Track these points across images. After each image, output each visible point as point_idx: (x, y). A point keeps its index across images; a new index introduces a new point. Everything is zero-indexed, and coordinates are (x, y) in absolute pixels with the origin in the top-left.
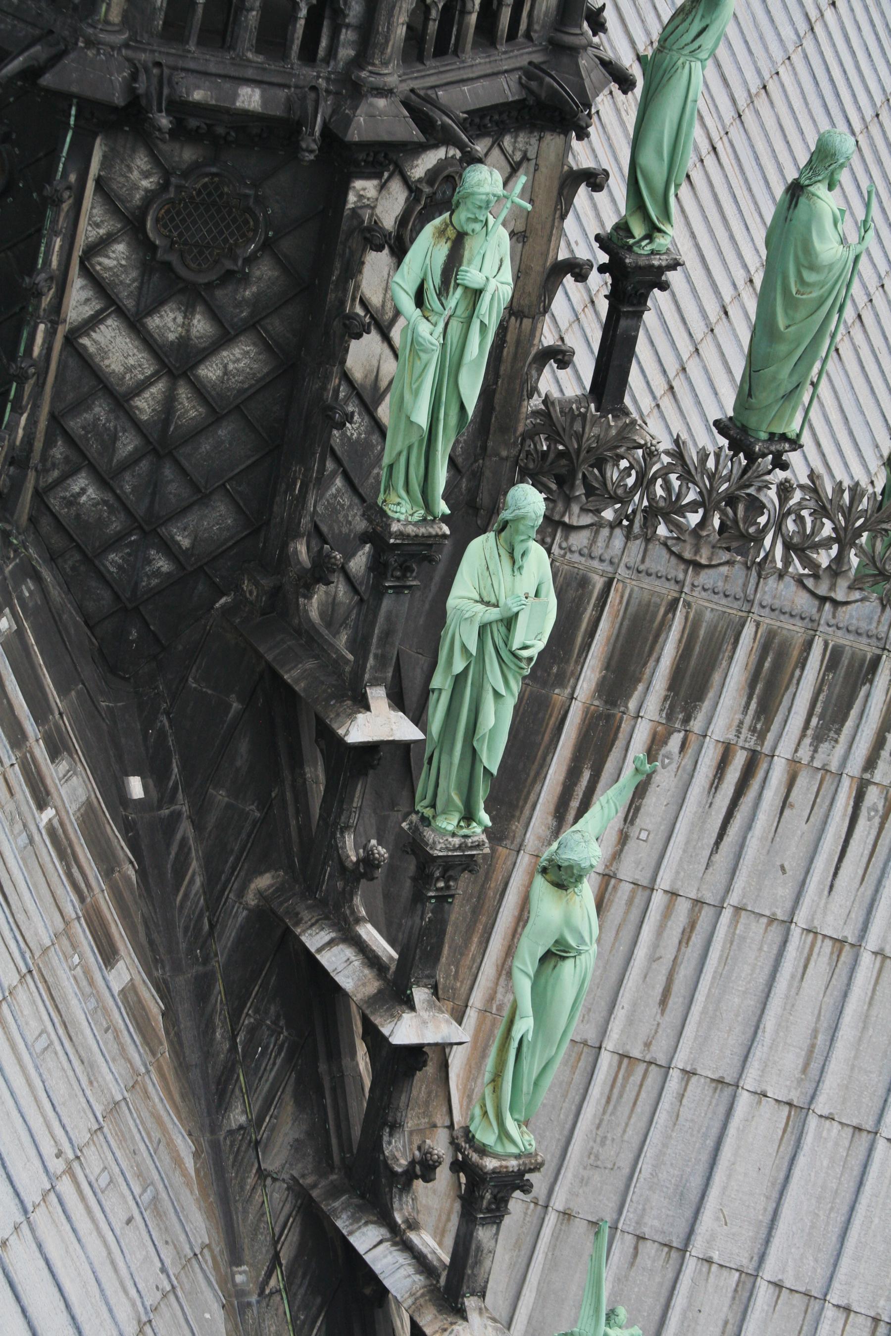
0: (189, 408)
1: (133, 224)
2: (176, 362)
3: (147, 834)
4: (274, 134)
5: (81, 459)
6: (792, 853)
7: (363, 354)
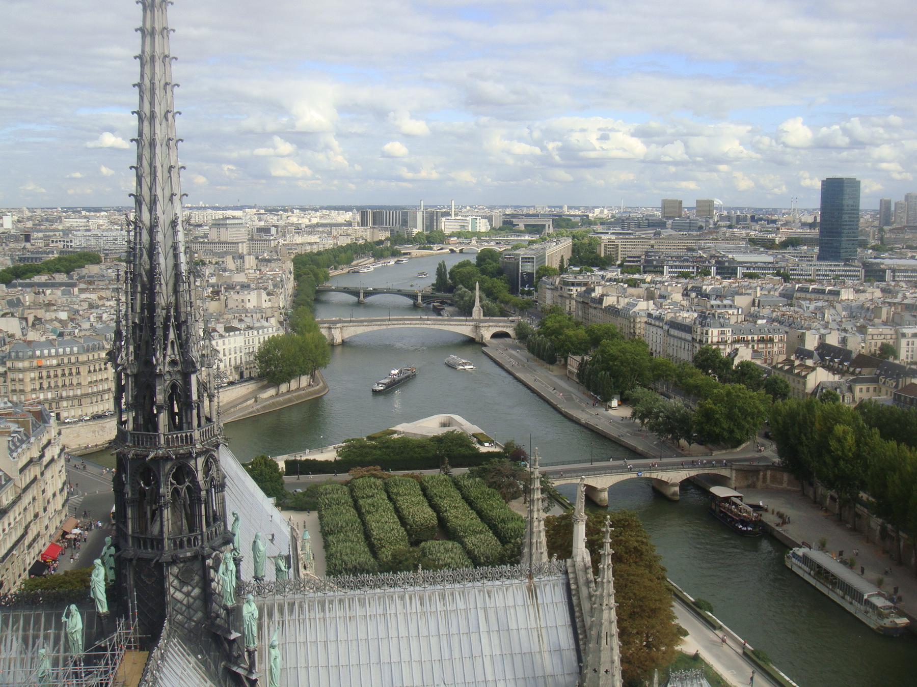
0: (191, 600)
1: (177, 577)
2: (188, 594)
3: (204, 662)
4: (195, 558)
5: (178, 612)
6: (293, 633)
7: (214, 584)
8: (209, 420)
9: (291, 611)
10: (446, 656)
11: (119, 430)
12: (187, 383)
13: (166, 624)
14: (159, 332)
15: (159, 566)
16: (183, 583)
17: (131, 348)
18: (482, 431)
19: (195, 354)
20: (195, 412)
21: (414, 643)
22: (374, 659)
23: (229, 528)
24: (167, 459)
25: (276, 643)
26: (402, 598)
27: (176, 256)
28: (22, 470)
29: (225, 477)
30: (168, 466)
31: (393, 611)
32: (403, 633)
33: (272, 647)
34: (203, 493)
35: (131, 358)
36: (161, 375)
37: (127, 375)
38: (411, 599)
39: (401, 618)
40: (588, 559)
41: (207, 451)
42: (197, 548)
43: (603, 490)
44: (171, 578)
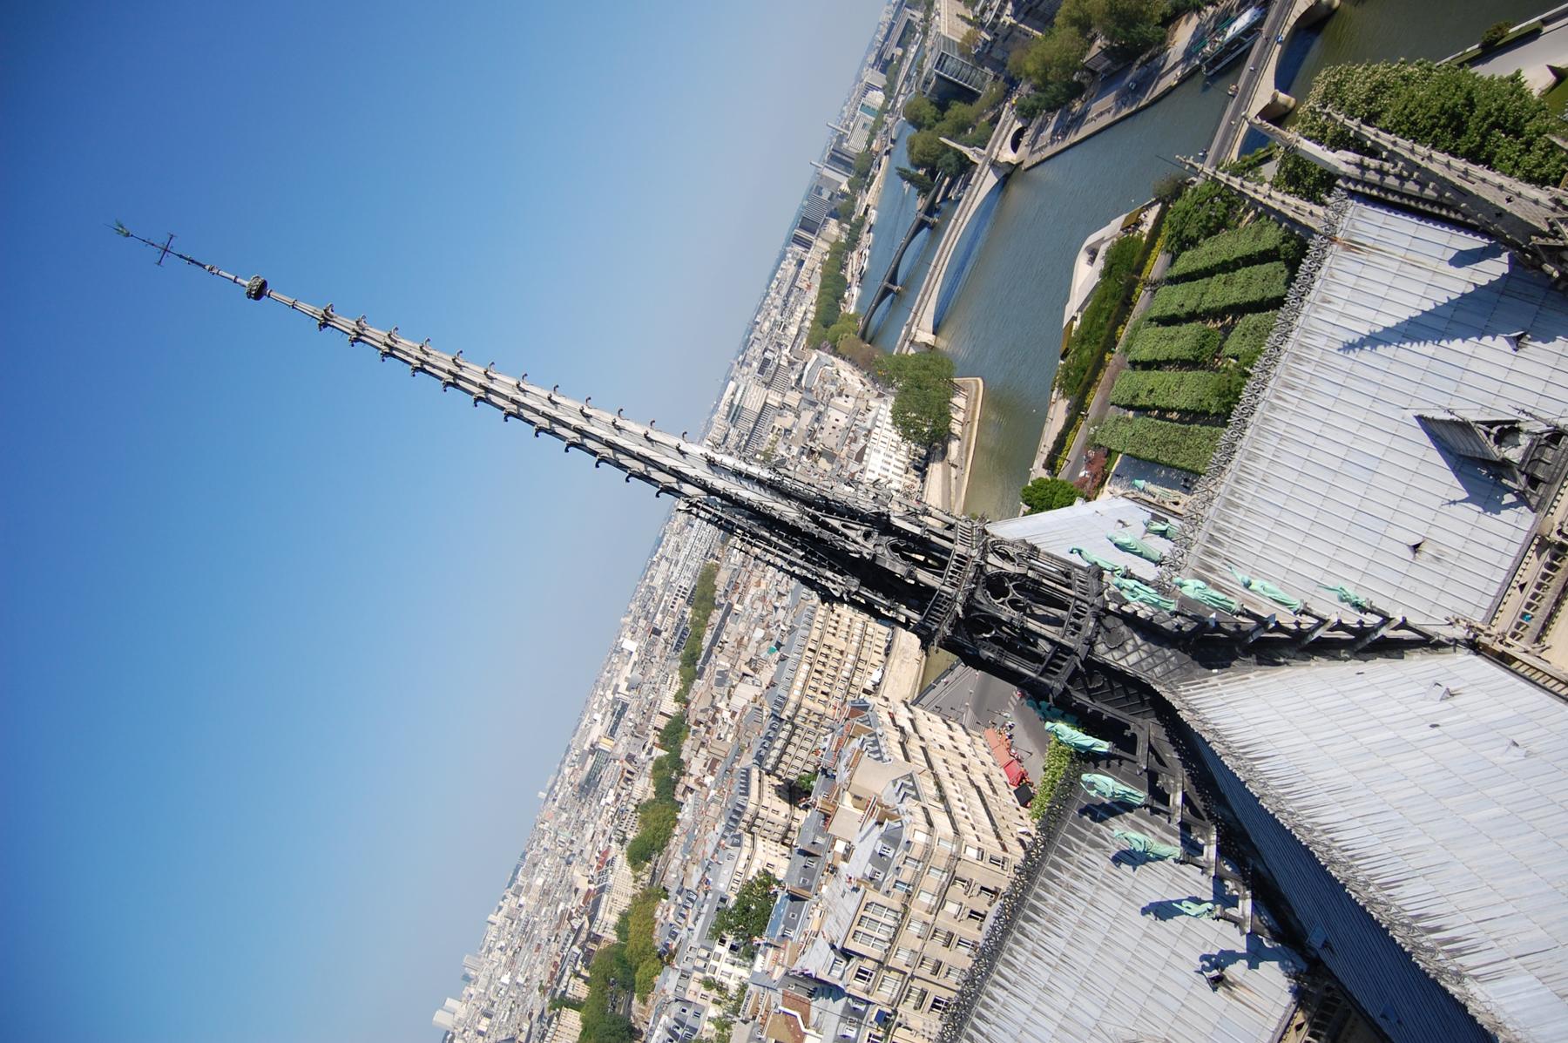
2: (1137, 648)
4: (1098, 619)
7: (1141, 614)
8: (950, 527)
9: (1219, 543)
10: (1372, 390)
11: (914, 631)
12: (898, 532)
13: (1157, 688)
14: (826, 535)
15: (1088, 663)
16: (1121, 646)
17: (829, 574)
18: (1123, 217)
19: (867, 506)
20: (934, 538)
21: (1336, 421)
22: (1328, 477)
23: (1086, 565)
24: (972, 593)
25: (1246, 579)
26: (1273, 407)
27: (749, 477)
28: (907, 758)
29: (1024, 541)
30: (978, 595)
31: (1283, 426)
32: (1315, 427)
33: (1247, 585)
34: (1030, 574)
35: (839, 579)
36: (875, 556)
37: (857, 593)
38: (1280, 398)
39: (1296, 421)
40: (1351, 156)
41: (985, 545)
42: (1090, 611)
43: (1275, 98)
44: (1109, 657)
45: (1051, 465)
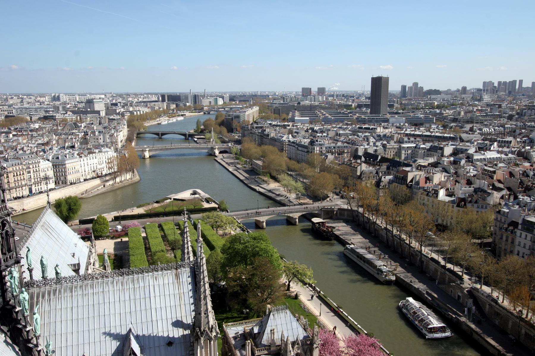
7: (8, 284)
10: (133, 309)
18: (209, 197)
21: (117, 304)
32: (112, 300)
45: (117, 219)
